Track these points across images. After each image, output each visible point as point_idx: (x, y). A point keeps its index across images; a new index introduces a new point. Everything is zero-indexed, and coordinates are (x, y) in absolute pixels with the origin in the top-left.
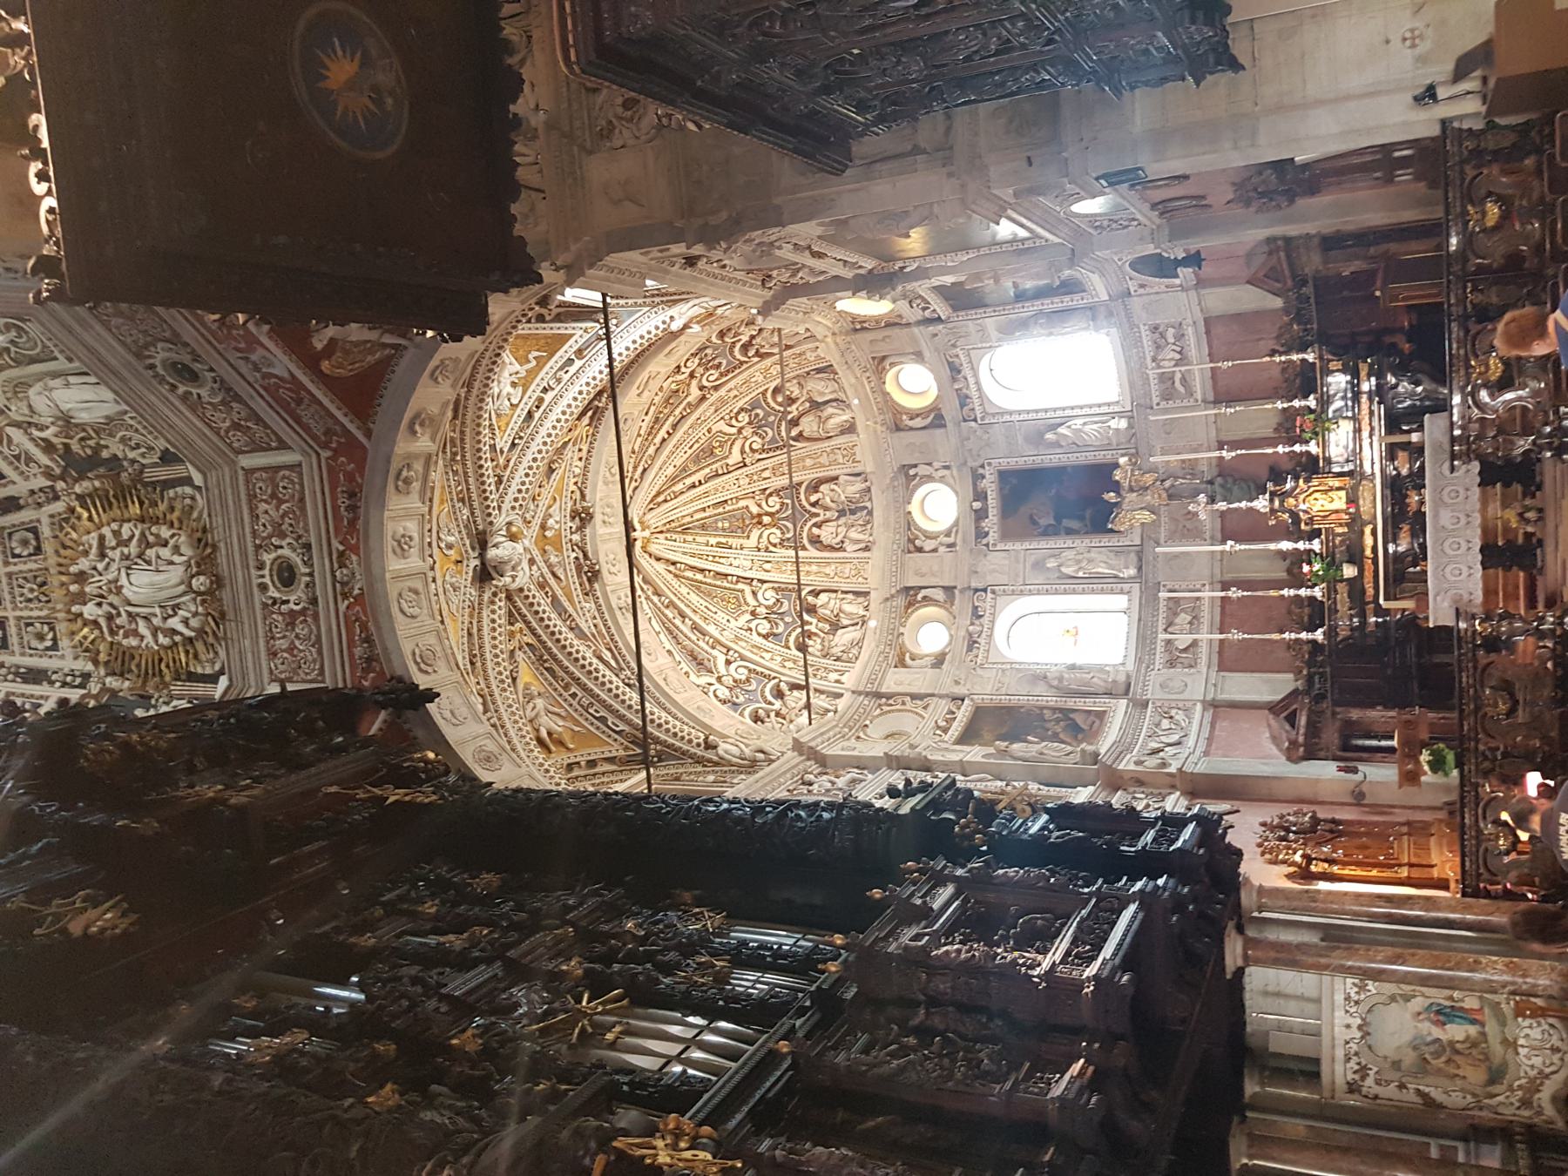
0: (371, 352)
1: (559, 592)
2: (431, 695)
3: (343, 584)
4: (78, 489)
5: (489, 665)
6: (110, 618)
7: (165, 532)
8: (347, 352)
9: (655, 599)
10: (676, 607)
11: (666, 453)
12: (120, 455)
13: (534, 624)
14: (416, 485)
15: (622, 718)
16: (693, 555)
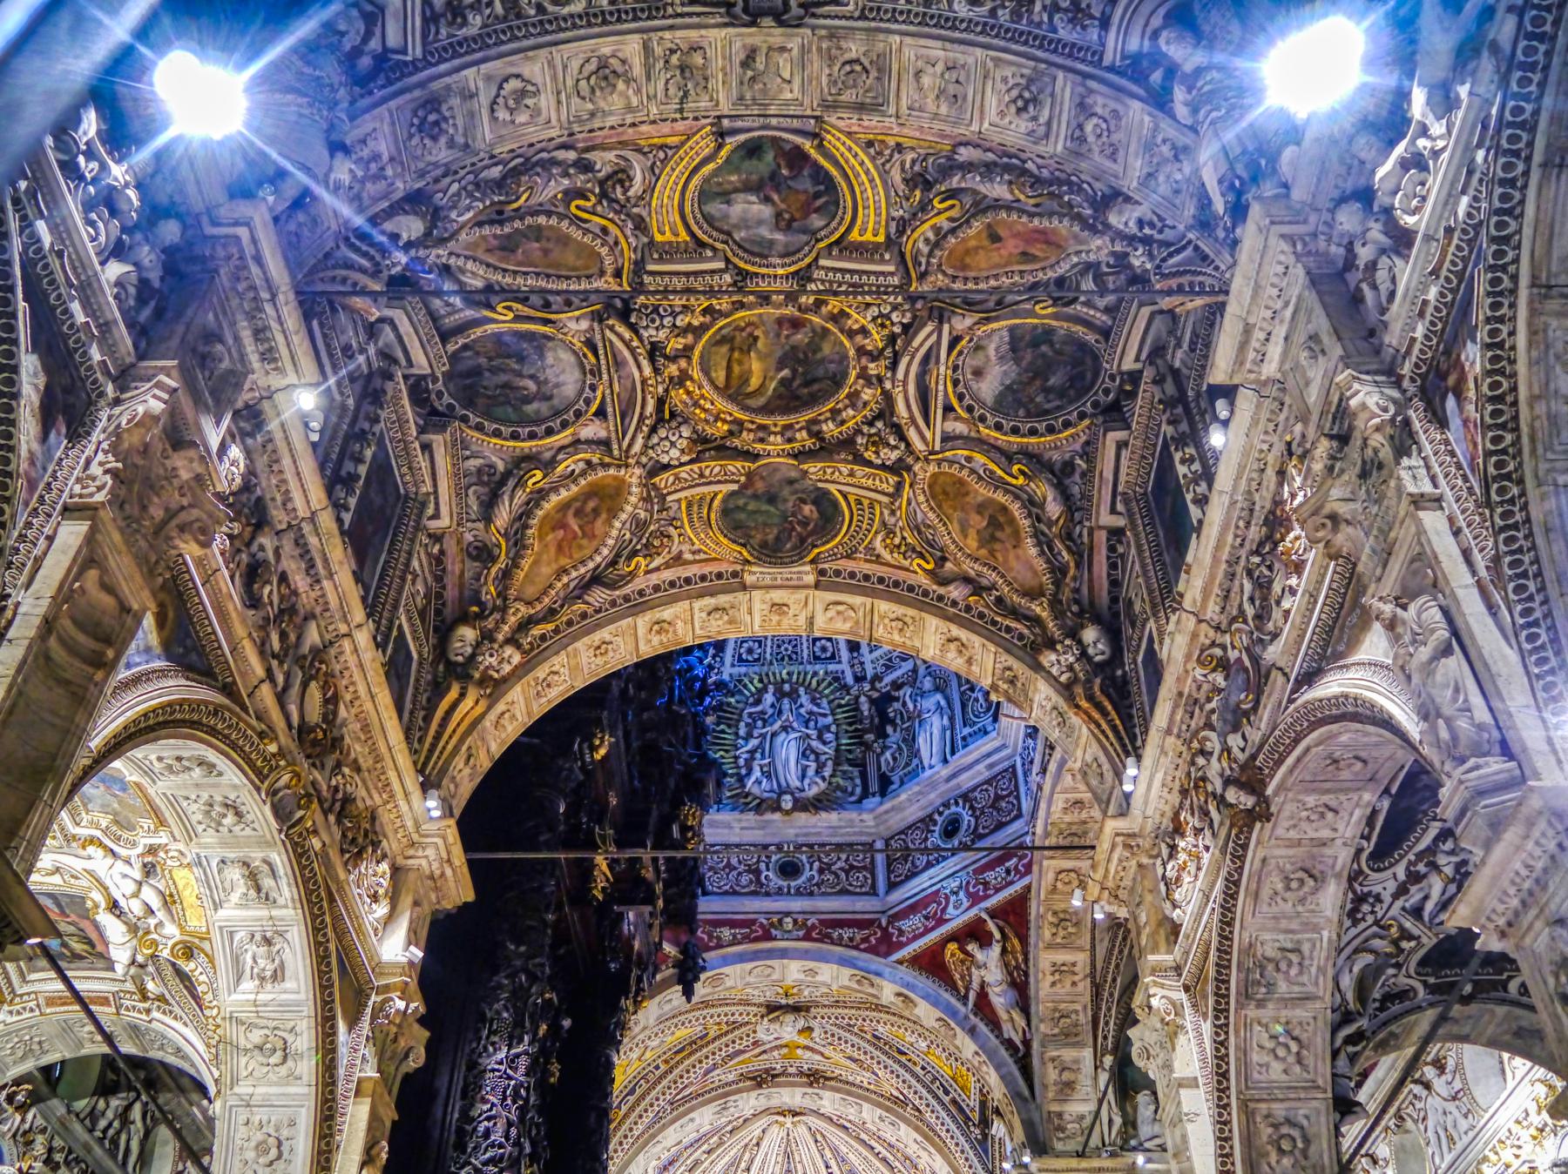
0: (962, 978)
1: (747, 1055)
2: (688, 993)
3: (780, 921)
4: (863, 699)
5: (697, 1014)
6: (763, 712)
7: (827, 772)
8: (962, 962)
9: (729, 1128)
10: (719, 1146)
11: (861, 1149)
12: (889, 742)
13: (724, 1040)
14: (856, 986)
15: (632, 1109)
16: (763, 1162)
